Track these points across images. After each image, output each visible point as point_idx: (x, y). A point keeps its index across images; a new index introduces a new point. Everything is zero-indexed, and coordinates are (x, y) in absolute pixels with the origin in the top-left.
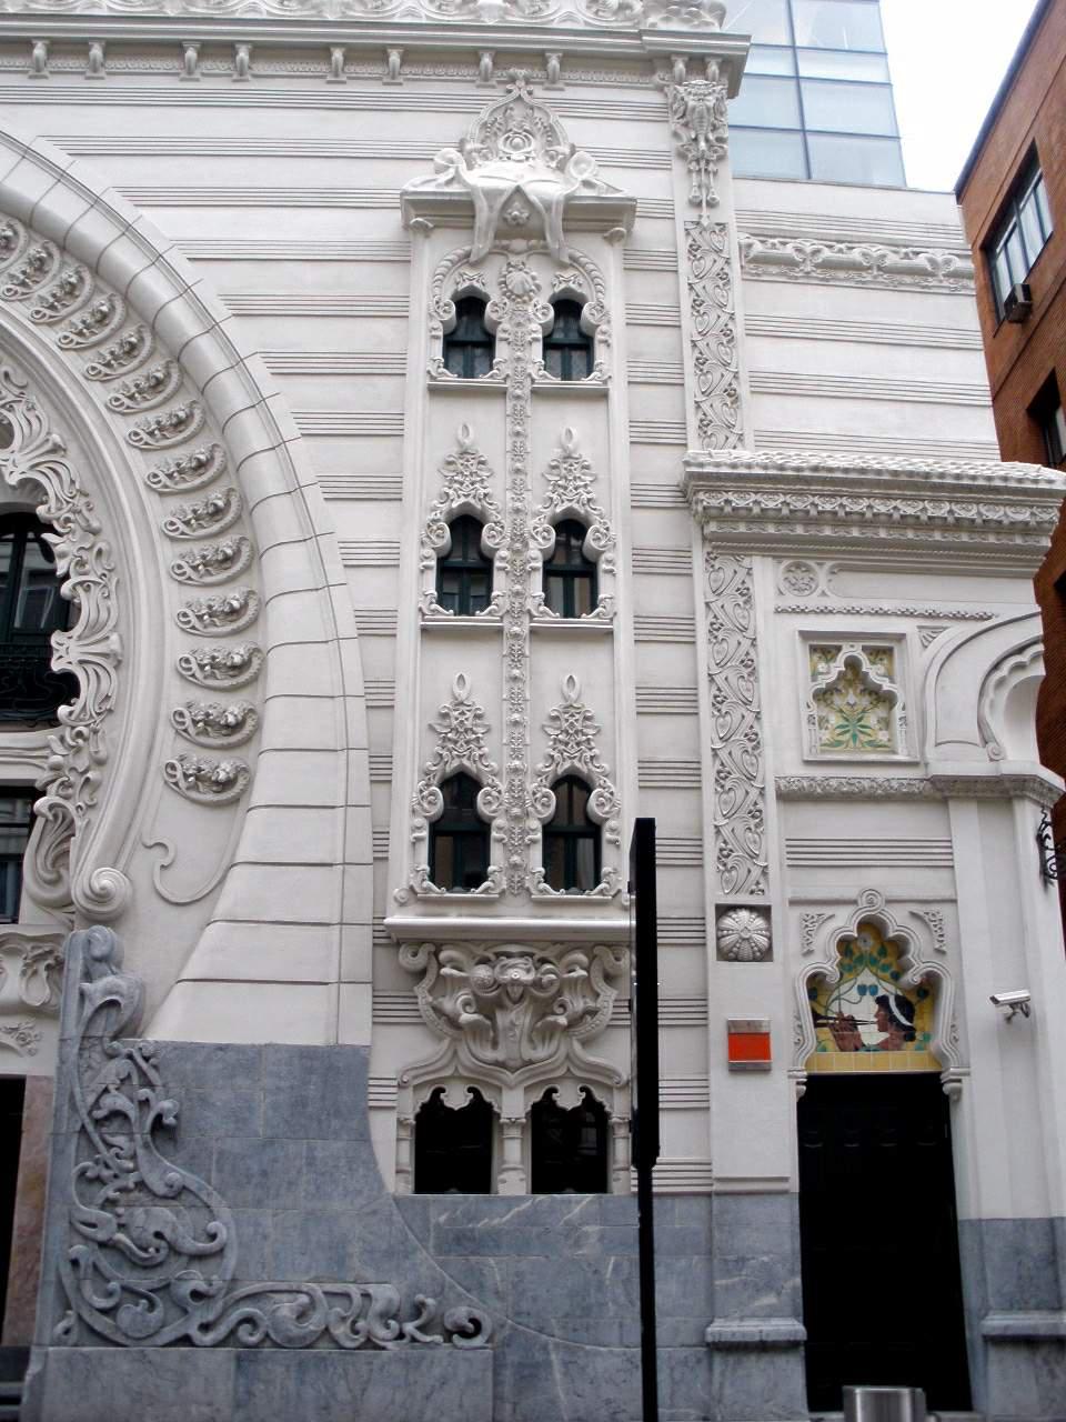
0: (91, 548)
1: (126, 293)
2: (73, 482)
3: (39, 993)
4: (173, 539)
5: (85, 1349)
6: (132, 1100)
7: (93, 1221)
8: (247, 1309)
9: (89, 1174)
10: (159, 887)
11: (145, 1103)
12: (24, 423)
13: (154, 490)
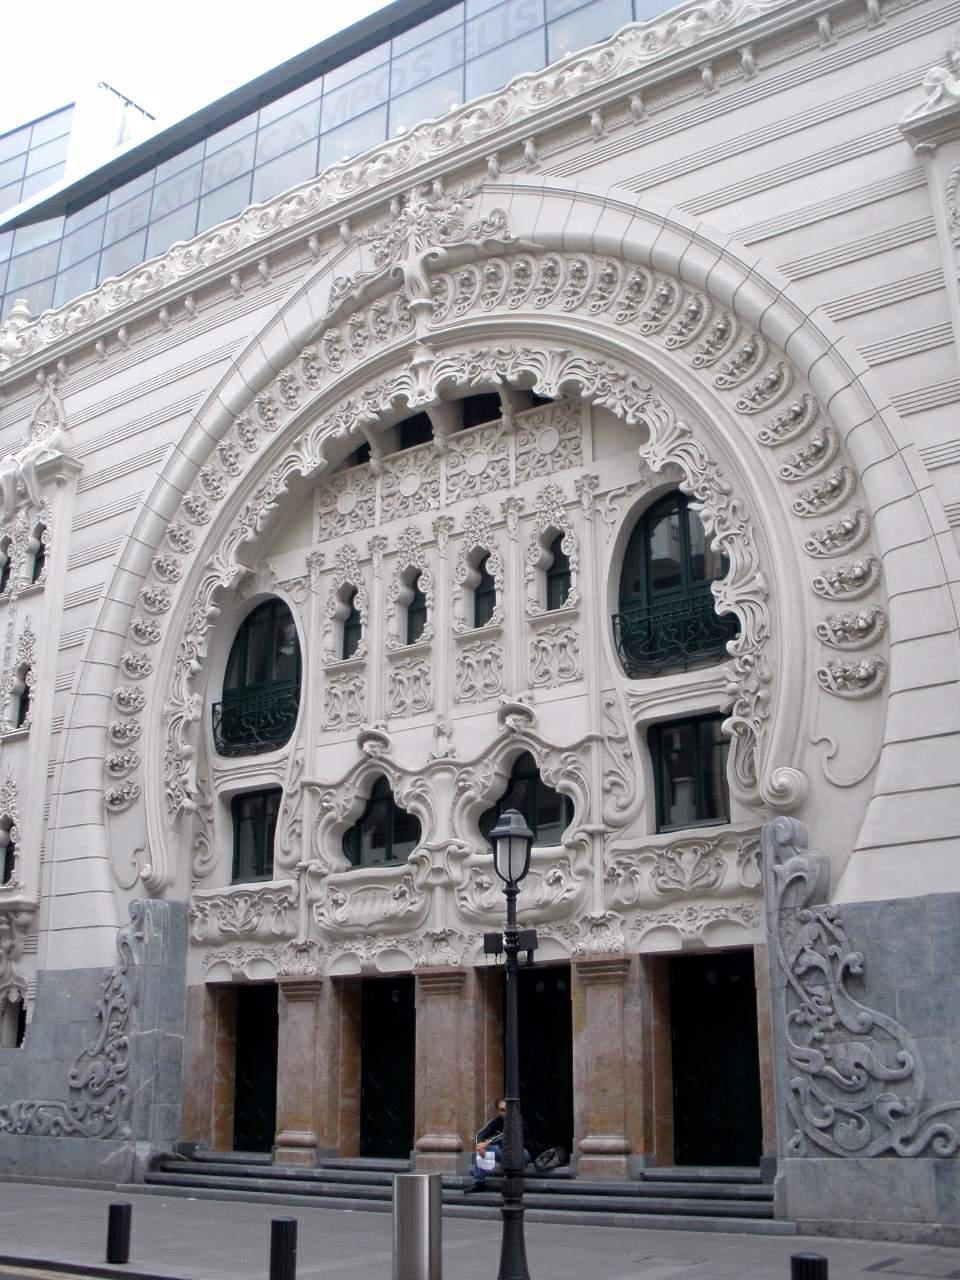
1: (706, 289)
2: (702, 457)
3: (753, 877)
4: (789, 483)
5: (814, 1160)
6: (824, 956)
7: (806, 1057)
8: (939, 1125)
9: (798, 1019)
10: (829, 776)
11: (834, 958)
12: (655, 419)
13: (766, 446)
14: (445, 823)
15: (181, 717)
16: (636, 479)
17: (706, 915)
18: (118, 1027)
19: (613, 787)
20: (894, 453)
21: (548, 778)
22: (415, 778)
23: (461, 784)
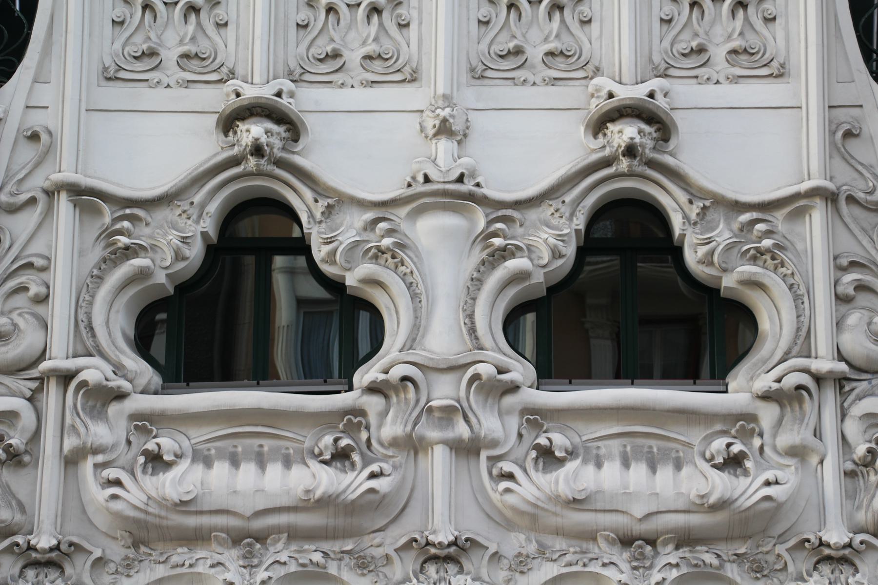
14: (441, 310)
21: (331, 258)
22: (369, 215)
23: (497, 242)
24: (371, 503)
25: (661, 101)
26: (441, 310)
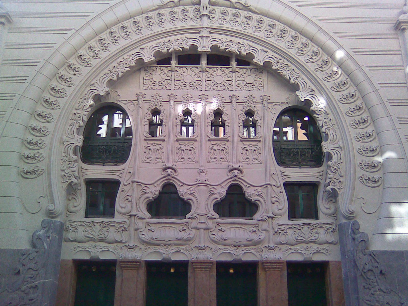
0: (328, 118)
7: (369, 300)
9: (366, 287)
14: (202, 204)
15: (74, 143)
16: (285, 102)
17: (313, 249)
18: (31, 278)
19: (274, 203)
20: (389, 116)
24: (189, 240)
25: (241, 167)
26: (202, 204)
